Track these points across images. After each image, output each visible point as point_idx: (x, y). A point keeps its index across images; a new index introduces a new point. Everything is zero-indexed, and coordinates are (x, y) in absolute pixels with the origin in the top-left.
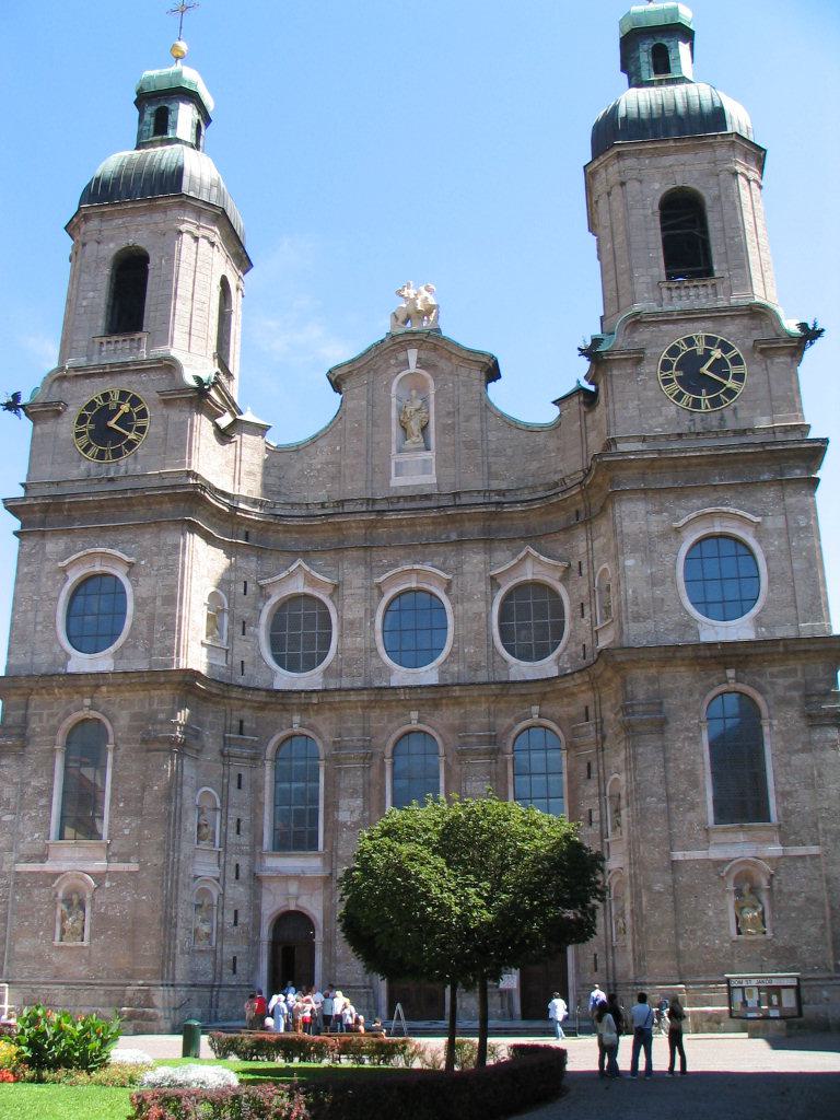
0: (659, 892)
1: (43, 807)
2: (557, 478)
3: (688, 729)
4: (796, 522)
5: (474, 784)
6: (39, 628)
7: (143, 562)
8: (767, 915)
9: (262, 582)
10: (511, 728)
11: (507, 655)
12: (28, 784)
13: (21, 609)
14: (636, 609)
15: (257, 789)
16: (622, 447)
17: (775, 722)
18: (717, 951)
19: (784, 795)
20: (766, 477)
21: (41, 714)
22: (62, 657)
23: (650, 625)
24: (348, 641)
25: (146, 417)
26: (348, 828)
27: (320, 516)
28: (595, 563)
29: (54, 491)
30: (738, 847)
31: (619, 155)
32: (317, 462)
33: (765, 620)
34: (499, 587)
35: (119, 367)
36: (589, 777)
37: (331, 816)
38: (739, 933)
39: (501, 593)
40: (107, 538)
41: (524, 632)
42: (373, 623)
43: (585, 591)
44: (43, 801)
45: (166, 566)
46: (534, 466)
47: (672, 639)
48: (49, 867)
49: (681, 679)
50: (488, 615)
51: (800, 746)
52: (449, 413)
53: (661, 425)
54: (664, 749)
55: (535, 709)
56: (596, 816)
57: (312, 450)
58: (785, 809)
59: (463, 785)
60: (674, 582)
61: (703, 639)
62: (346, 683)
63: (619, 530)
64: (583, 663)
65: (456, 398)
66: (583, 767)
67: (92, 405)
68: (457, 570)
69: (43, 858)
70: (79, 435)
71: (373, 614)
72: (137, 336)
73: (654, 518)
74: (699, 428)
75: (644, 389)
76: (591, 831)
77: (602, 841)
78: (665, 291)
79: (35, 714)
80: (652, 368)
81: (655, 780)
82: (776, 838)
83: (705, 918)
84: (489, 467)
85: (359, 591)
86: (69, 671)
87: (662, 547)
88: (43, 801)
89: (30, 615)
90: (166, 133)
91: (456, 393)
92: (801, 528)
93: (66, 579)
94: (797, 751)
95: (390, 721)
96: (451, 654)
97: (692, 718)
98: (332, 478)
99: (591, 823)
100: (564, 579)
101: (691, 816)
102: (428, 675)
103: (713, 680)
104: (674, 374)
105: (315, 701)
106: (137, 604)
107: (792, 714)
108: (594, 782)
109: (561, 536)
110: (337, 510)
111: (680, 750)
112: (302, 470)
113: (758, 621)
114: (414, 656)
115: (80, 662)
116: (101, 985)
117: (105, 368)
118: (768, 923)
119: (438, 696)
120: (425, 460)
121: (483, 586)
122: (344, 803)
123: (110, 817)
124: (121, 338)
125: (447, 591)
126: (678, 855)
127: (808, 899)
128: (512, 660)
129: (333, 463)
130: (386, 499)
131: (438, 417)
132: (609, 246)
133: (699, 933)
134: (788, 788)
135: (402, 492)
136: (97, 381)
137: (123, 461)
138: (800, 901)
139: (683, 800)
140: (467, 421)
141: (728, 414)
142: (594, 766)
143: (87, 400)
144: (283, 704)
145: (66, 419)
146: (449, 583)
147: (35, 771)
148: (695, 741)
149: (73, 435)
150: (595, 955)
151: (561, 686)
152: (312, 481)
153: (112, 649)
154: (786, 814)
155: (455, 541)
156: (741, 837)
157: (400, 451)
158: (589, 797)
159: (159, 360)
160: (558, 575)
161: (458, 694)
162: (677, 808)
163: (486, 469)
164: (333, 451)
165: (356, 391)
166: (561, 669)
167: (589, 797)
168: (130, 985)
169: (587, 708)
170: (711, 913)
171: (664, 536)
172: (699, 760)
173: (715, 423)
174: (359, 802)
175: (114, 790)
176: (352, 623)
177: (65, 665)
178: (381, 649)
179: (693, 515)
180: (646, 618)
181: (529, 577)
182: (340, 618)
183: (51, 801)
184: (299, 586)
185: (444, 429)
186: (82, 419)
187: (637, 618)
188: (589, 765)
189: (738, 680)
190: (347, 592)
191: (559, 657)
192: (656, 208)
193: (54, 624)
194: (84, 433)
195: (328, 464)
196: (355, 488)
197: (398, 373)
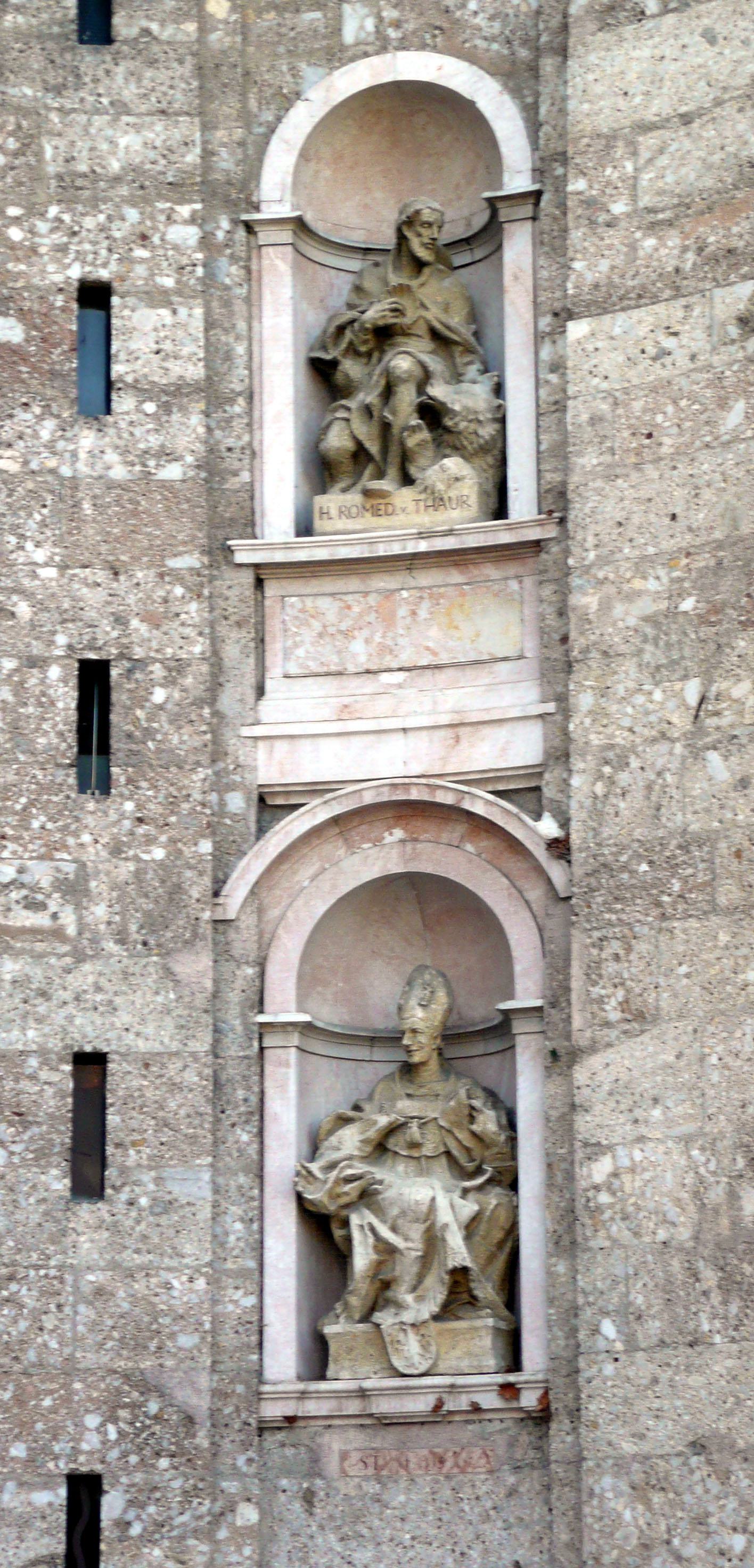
56: (145, 336)
77: (220, 554)
150: (84, 1491)
158: (76, 188)
167: (76, 188)
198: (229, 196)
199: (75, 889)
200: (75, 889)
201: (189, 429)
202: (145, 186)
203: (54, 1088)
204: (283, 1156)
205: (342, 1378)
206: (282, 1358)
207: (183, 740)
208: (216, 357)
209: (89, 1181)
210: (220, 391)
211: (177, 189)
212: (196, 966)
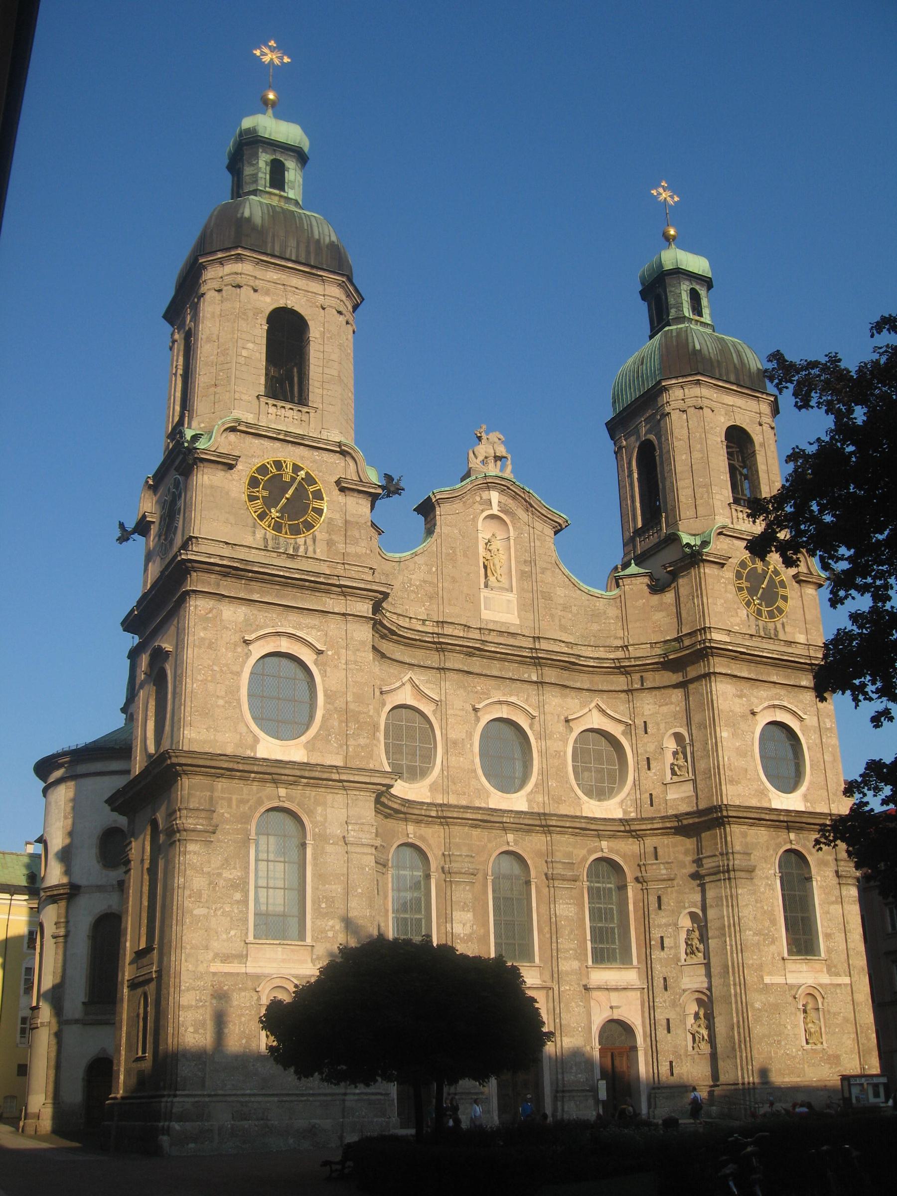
0: (759, 1009)
1: (238, 902)
2: (619, 643)
3: (767, 878)
4: (824, 723)
5: (562, 906)
6: (221, 702)
7: (330, 653)
8: (823, 1030)
9: (385, 689)
10: (585, 859)
11: (579, 793)
12: (220, 875)
13: (199, 678)
14: (731, 774)
15: (386, 897)
16: (716, 636)
17: (819, 879)
18: (794, 1057)
19: (828, 936)
20: (804, 683)
21: (230, 800)
22: (250, 740)
23: (739, 789)
24: (453, 760)
25: (323, 499)
26: (460, 939)
27: (433, 634)
28: (662, 726)
29: (226, 552)
30: (803, 974)
31: (698, 382)
32: (417, 577)
33: (809, 797)
34: (571, 730)
35: (295, 437)
36: (660, 908)
37: (443, 928)
38: (807, 1043)
39: (574, 735)
40: (290, 618)
41: (586, 774)
42: (471, 745)
43: (651, 748)
44: (238, 896)
45: (356, 662)
46: (595, 627)
47: (754, 803)
48: (252, 967)
49: (760, 835)
50: (565, 753)
51: (834, 899)
52: (525, 561)
53: (738, 625)
54: (754, 893)
55: (604, 844)
57: (411, 564)
58: (828, 947)
59: (552, 906)
60: (753, 756)
61: (774, 806)
62: (453, 800)
63: (715, 705)
64: (648, 812)
65: (532, 550)
66: (653, 900)
67: (263, 469)
68: (540, 706)
69: (242, 957)
70: (252, 498)
71: (470, 735)
72: (305, 409)
73: (737, 700)
74: (762, 634)
75: (726, 591)
76: (663, 954)
78: (733, 510)
79: (223, 798)
80: (728, 574)
81: (751, 917)
82: (825, 969)
83: (786, 1032)
84: (560, 620)
85: (460, 713)
86: (259, 755)
87: (743, 726)
88: (238, 896)
89: (211, 687)
90: (284, 190)
91: (532, 544)
92: (828, 729)
93: (248, 655)
94: (833, 903)
95: (489, 841)
96: (536, 785)
97: (770, 869)
98: (431, 598)
99: (663, 948)
100: (624, 733)
101: (773, 948)
102: (518, 802)
103: (780, 840)
104: (745, 584)
105: (434, 814)
106: (326, 695)
107: (830, 873)
108: (662, 913)
109: (623, 695)
110: (436, 630)
111: (763, 893)
112: (403, 583)
113: (805, 797)
114: (508, 785)
115: (269, 748)
116: (313, 1095)
117: (279, 434)
118: (823, 1036)
119: (537, 822)
120: (509, 601)
121: (561, 727)
122: (457, 915)
123: (313, 918)
124: (288, 406)
125: (531, 726)
126: (767, 980)
127: (844, 1018)
128: (585, 798)
129: (430, 583)
130: (480, 629)
131: (517, 562)
132: (684, 457)
133: (783, 1043)
134: (829, 931)
135: (491, 627)
136: (266, 443)
137: (300, 540)
138: (839, 1020)
139: (767, 934)
140: (543, 573)
141: (779, 626)
142: (664, 899)
143: (258, 462)
144: (405, 813)
145: (235, 477)
146: (533, 717)
147: (226, 860)
148: (771, 887)
149: (245, 497)
150: (671, 1063)
151: (638, 827)
152: (413, 596)
153: (303, 739)
154: (829, 951)
155: (536, 682)
156: (804, 967)
157: (486, 586)
158: (659, 926)
159: (340, 444)
160: (621, 728)
161: (554, 823)
162: (764, 940)
163: (557, 621)
164: (430, 572)
165: (449, 517)
166: (625, 812)
167: (659, 926)
168: (345, 1094)
169: (655, 848)
170: (789, 1027)
171: (743, 716)
172: (776, 904)
173: (772, 632)
174: (470, 915)
175: (315, 889)
176: (455, 743)
177: (253, 748)
178: (480, 772)
179: (766, 704)
180: (738, 783)
181: (596, 726)
182: (445, 737)
183: (246, 896)
184: (406, 696)
185: (523, 575)
186: (253, 482)
187: (732, 782)
188: (659, 898)
189: (797, 843)
190: (449, 712)
191: (622, 801)
192: (723, 439)
193: (238, 701)
194: (257, 498)
195: (425, 581)
196: (451, 612)
197: (483, 511)
198: (676, 925)
199: (665, 1002)
200: (665, 1002)
201: (673, 951)
202: (667, 925)
203: (664, 1022)
204: (689, 1027)
205: (696, 1049)
206: (690, 1048)
207: (674, 985)
208: (675, 943)
209: (669, 1032)
210: (676, 946)
211: (670, 925)
212: (678, 1009)
